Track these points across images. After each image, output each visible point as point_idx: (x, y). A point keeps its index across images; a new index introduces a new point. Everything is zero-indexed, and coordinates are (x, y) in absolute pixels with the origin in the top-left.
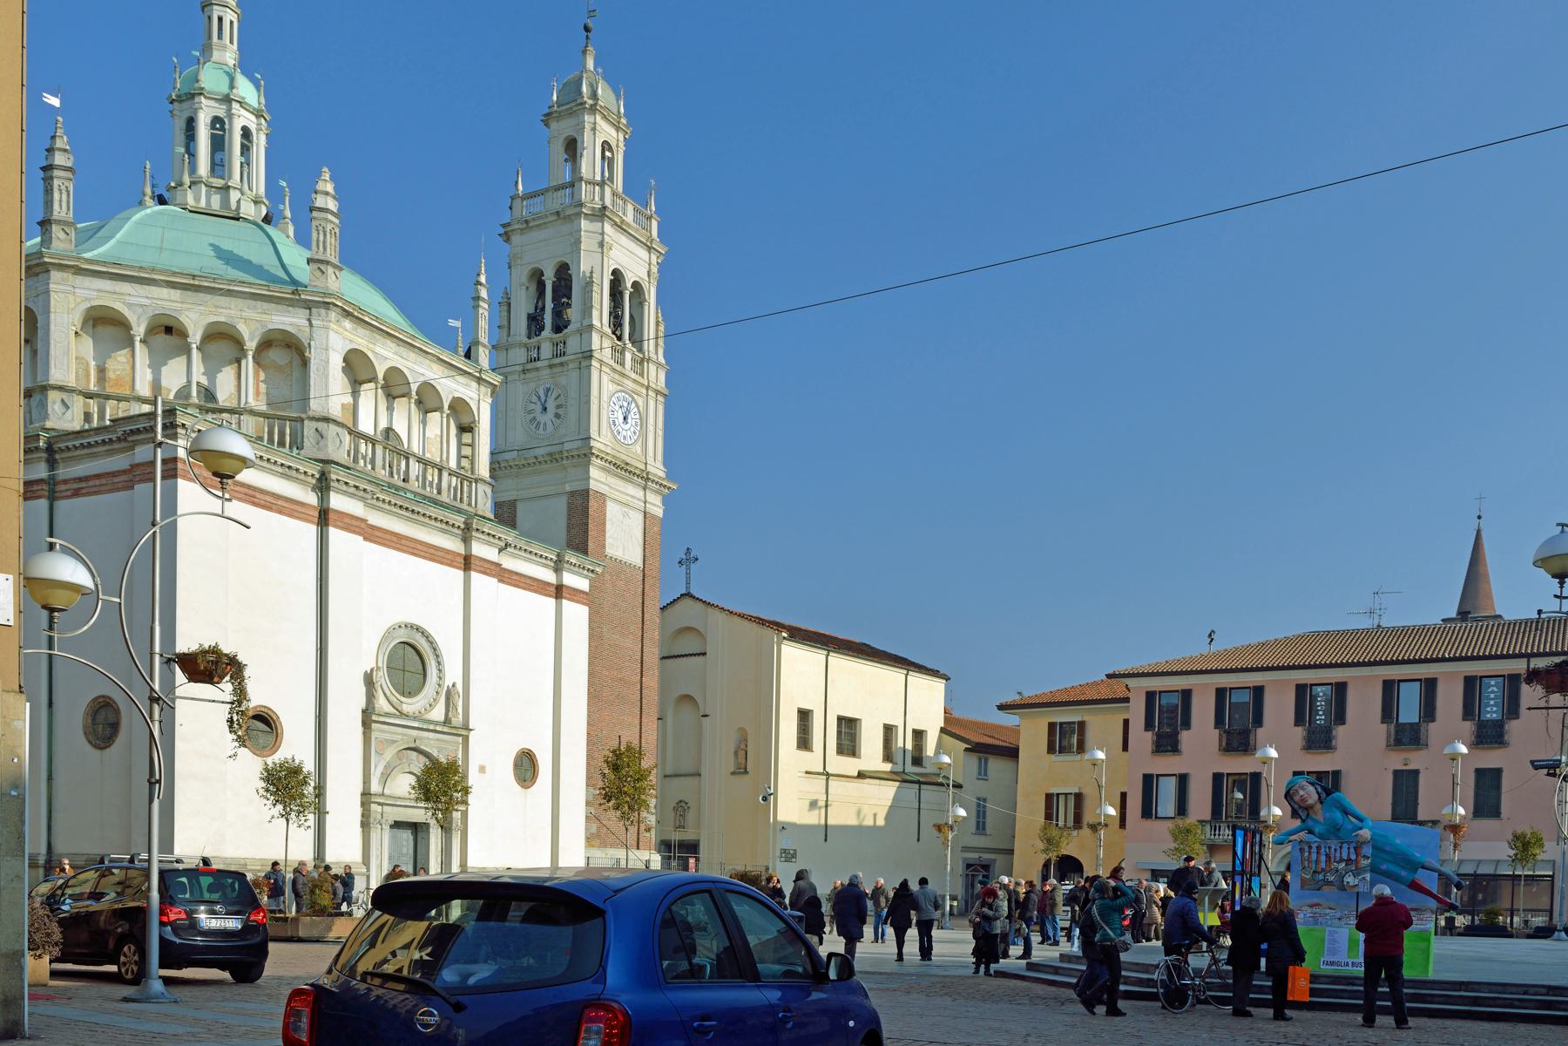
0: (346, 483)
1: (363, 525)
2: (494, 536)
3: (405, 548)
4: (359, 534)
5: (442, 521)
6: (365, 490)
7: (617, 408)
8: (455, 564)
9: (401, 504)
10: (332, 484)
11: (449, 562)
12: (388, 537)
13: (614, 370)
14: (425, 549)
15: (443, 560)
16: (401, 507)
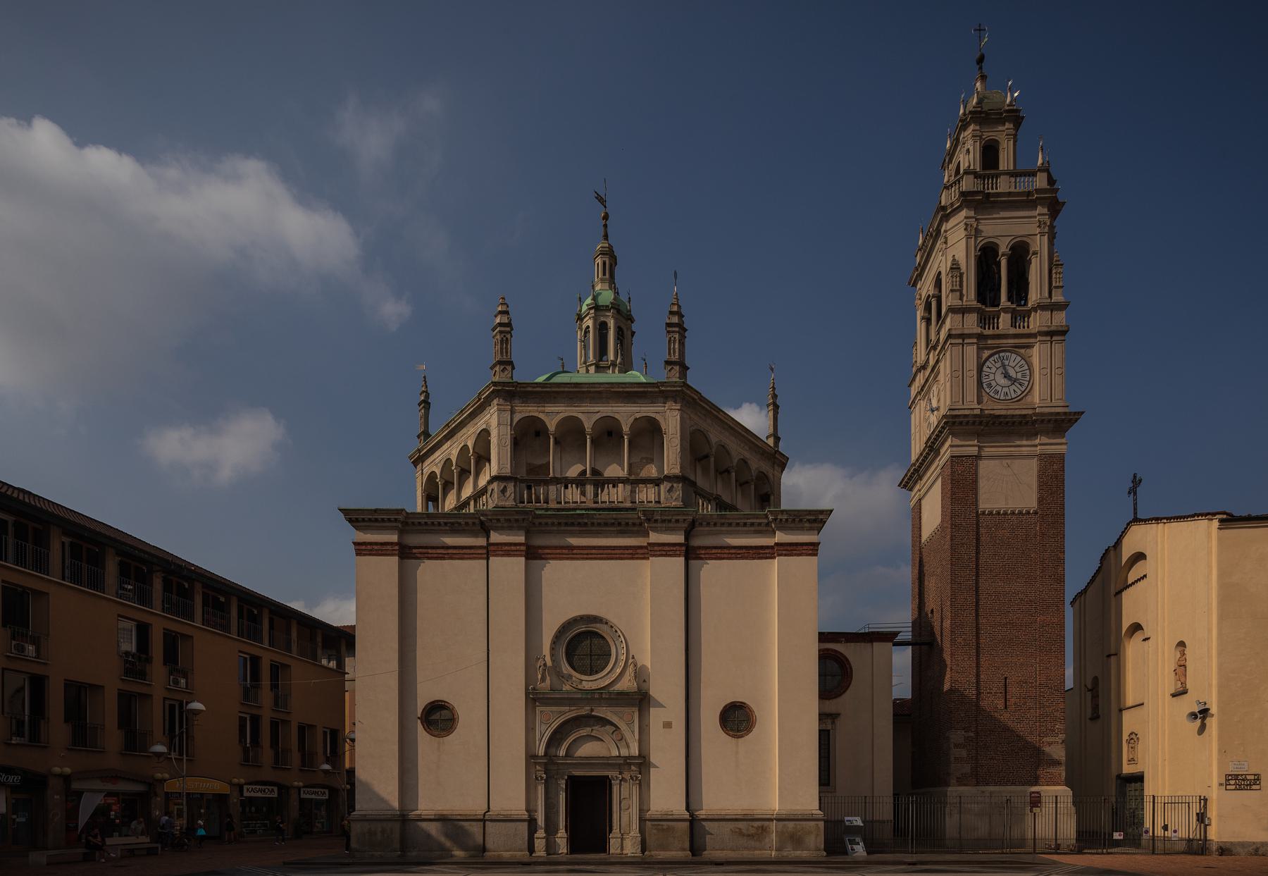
0: (498, 520)
1: (523, 548)
2: (670, 521)
3: (578, 556)
4: (521, 556)
5: (614, 523)
6: (517, 521)
7: (994, 370)
8: (636, 556)
9: (565, 521)
10: (487, 524)
11: (630, 556)
12: (558, 551)
13: (980, 337)
14: (601, 552)
15: (622, 556)
16: (566, 524)
